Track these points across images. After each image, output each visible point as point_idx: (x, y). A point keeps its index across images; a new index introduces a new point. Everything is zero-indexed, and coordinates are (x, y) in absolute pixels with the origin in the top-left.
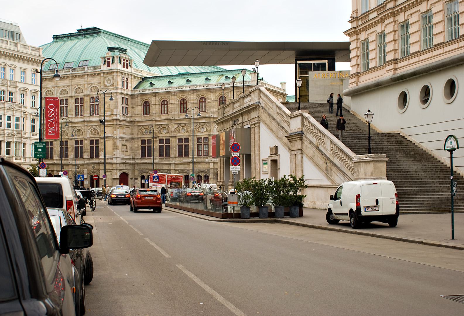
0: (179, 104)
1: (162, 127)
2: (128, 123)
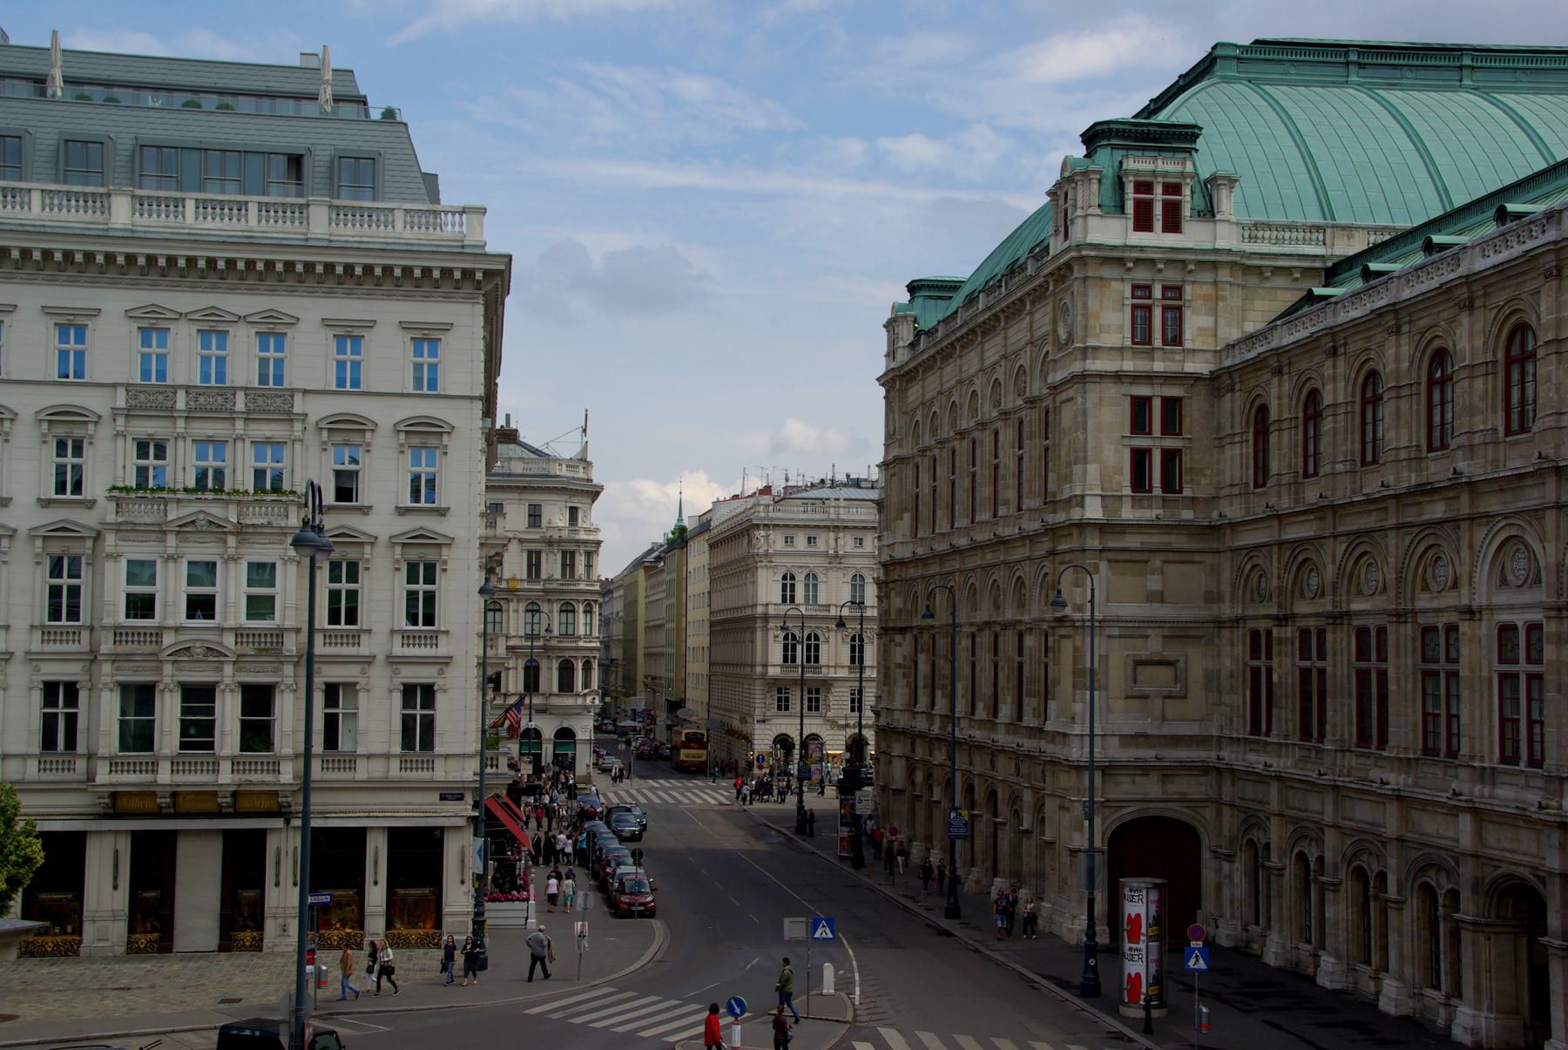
0: (1358, 407)
1: (1300, 559)
2: (1183, 539)
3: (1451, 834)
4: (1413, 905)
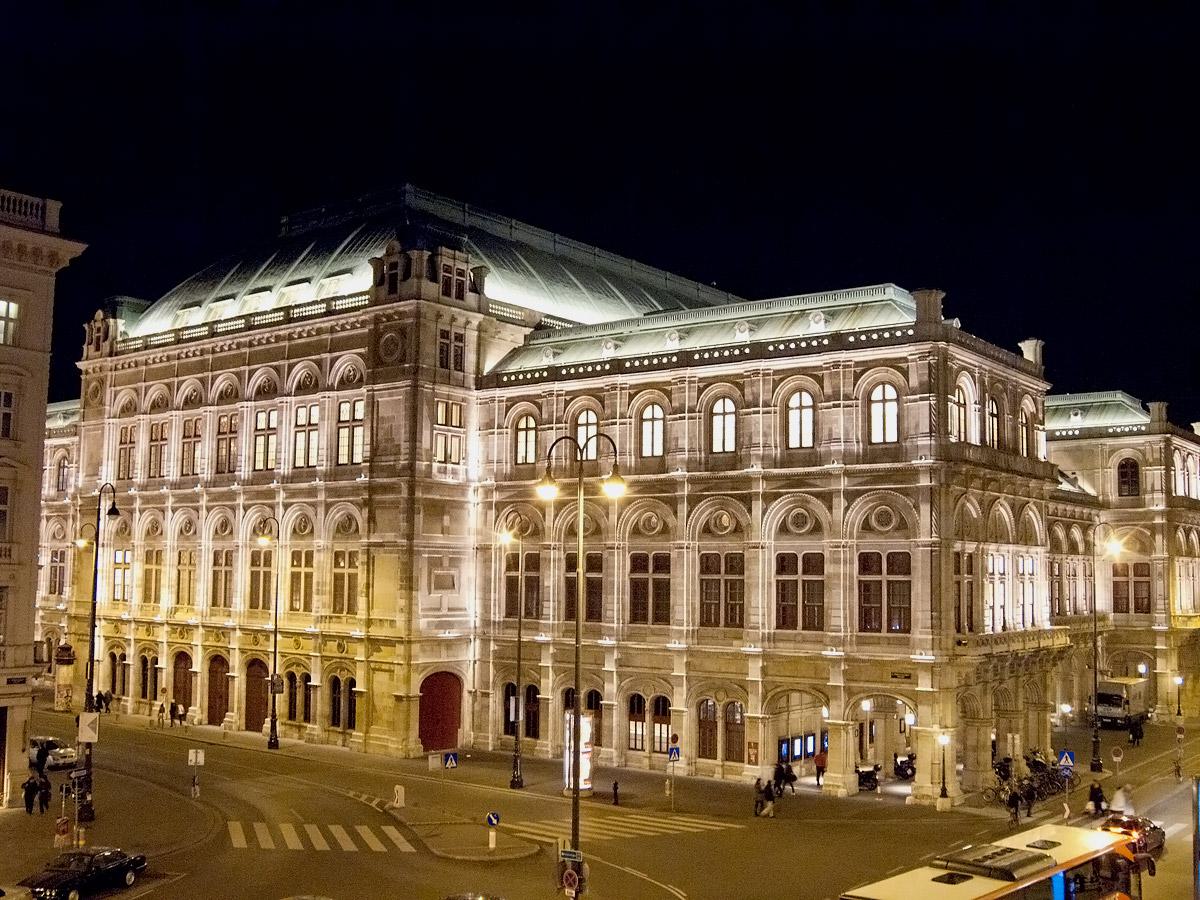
3: (733, 669)
4: (694, 710)
